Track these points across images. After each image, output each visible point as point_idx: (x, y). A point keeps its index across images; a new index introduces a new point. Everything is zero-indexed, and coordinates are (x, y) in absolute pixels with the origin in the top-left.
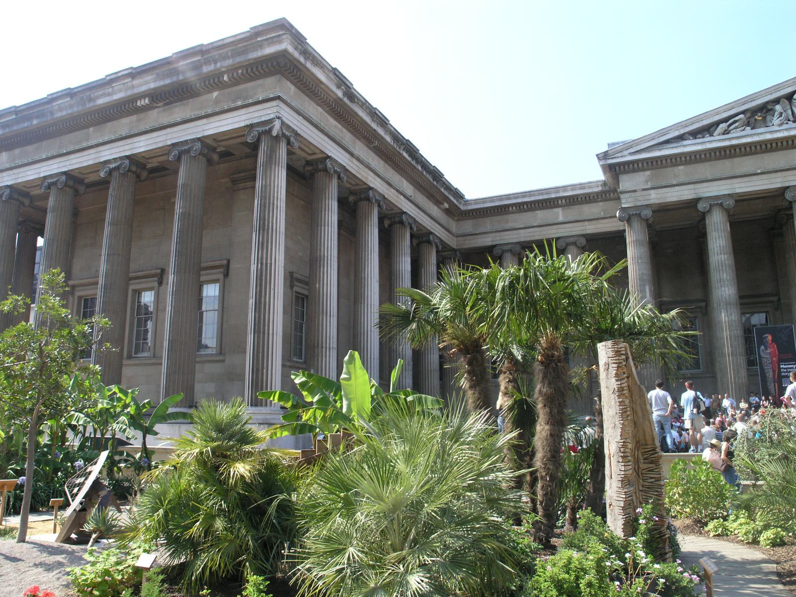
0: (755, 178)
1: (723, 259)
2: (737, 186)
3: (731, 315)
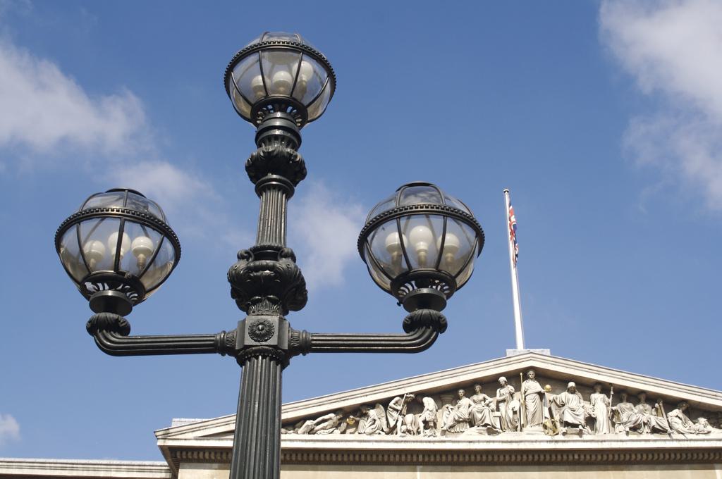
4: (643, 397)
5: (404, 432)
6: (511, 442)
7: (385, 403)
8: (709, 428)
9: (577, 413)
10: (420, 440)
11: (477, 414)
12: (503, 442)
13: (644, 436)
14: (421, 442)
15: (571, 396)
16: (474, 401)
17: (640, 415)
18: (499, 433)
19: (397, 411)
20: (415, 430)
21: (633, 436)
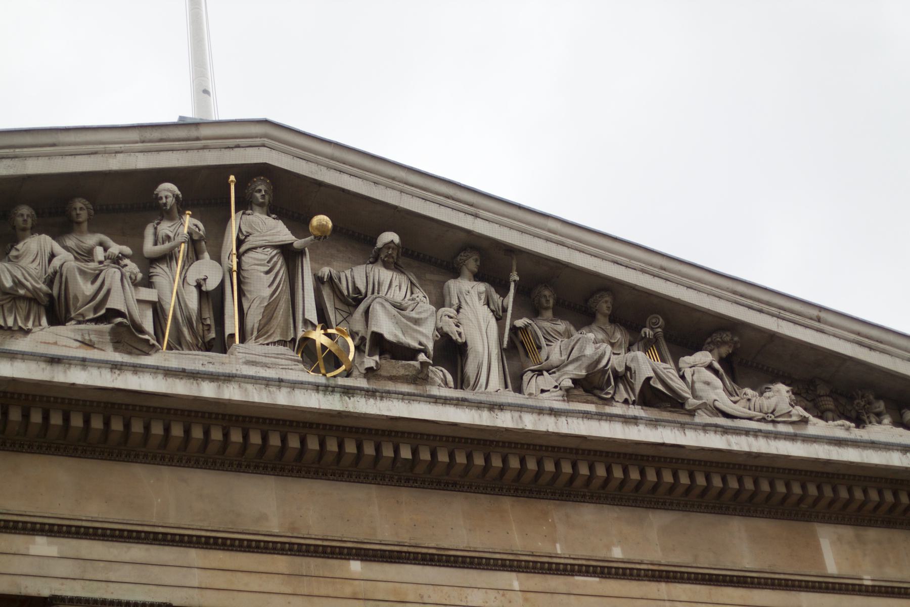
4: (604, 305)
9: (414, 315)
11: (79, 279)
12: (169, 373)
13: (618, 409)
15: (385, 275)
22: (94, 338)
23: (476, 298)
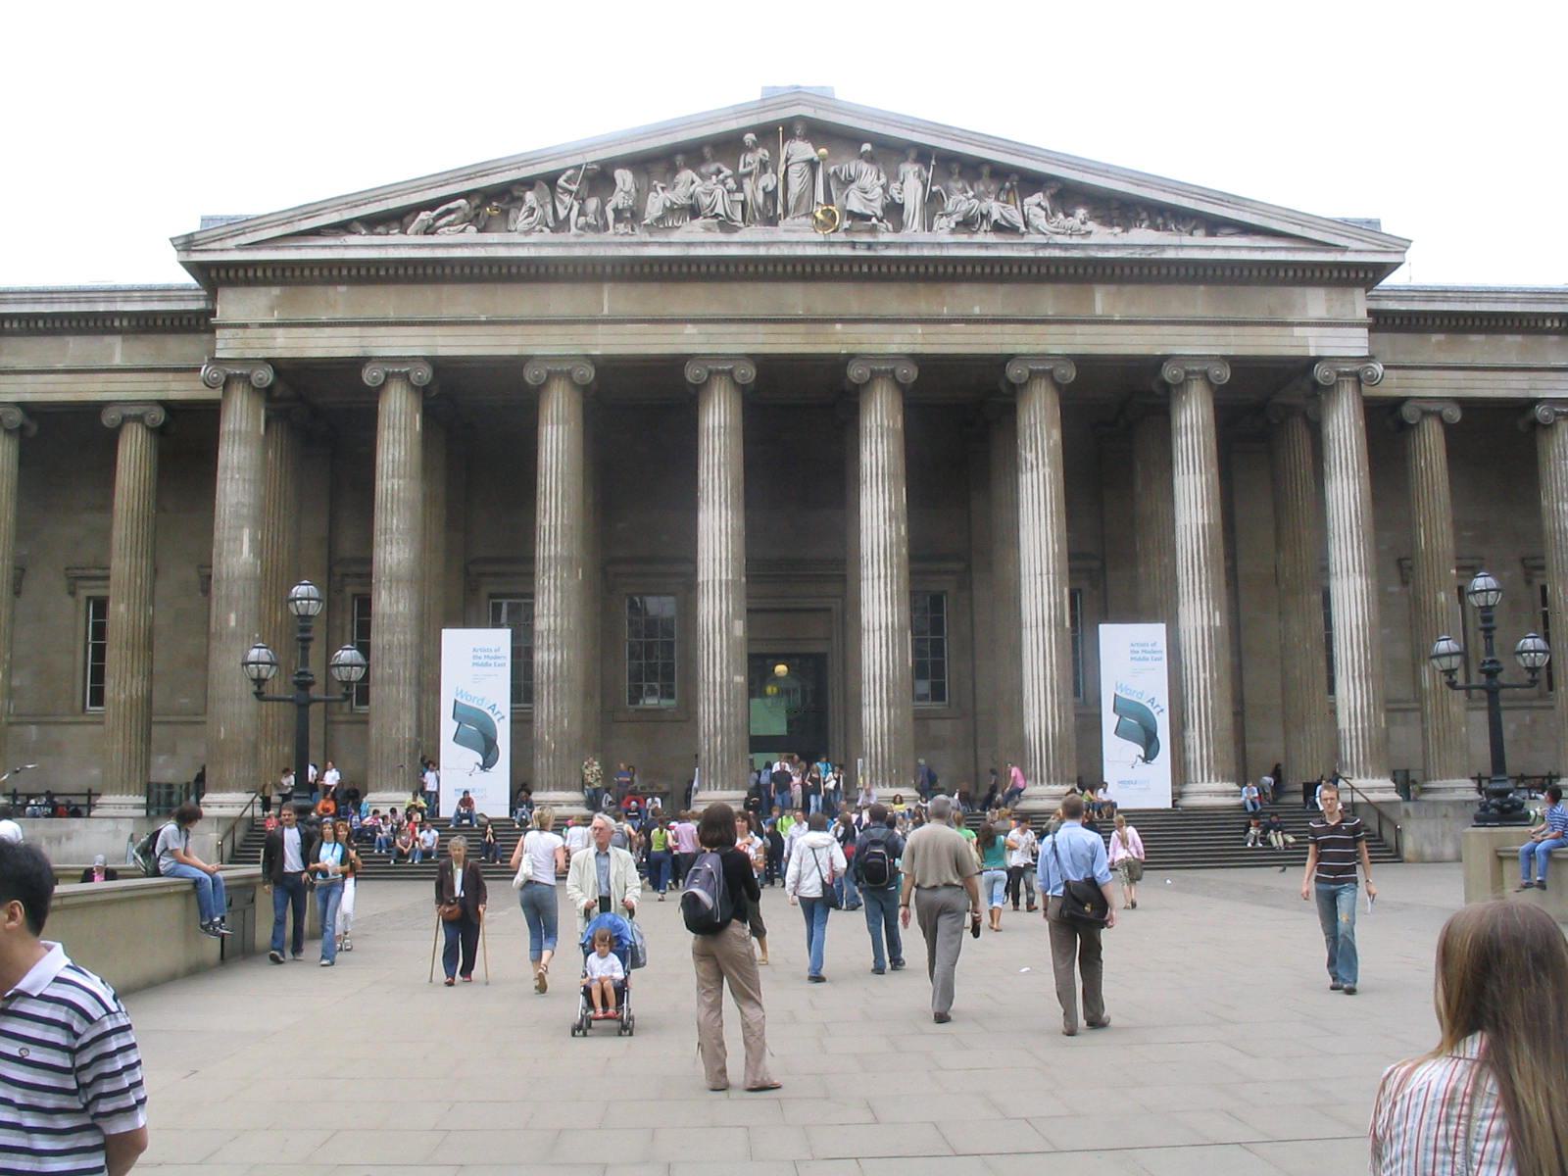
0: (475, 330)
1: (396, 487)
2: (440, 341)
3: (397, 602)
4: (986, 170)
5: (581, 229)
6: (756, 244)
7: (551, 180)
8: (1091, 225)
9: (868, 196)
10: (608, 240)
13: (979, 238)
14: (608, 244)
15: (865, 166)
16: (702, 177)
17: (975, 201)
18: (740, 228)
19: (570, 192)
20: (601, 223)
21: (963, 238)
22: (710, 226)
23: (912, 175)
